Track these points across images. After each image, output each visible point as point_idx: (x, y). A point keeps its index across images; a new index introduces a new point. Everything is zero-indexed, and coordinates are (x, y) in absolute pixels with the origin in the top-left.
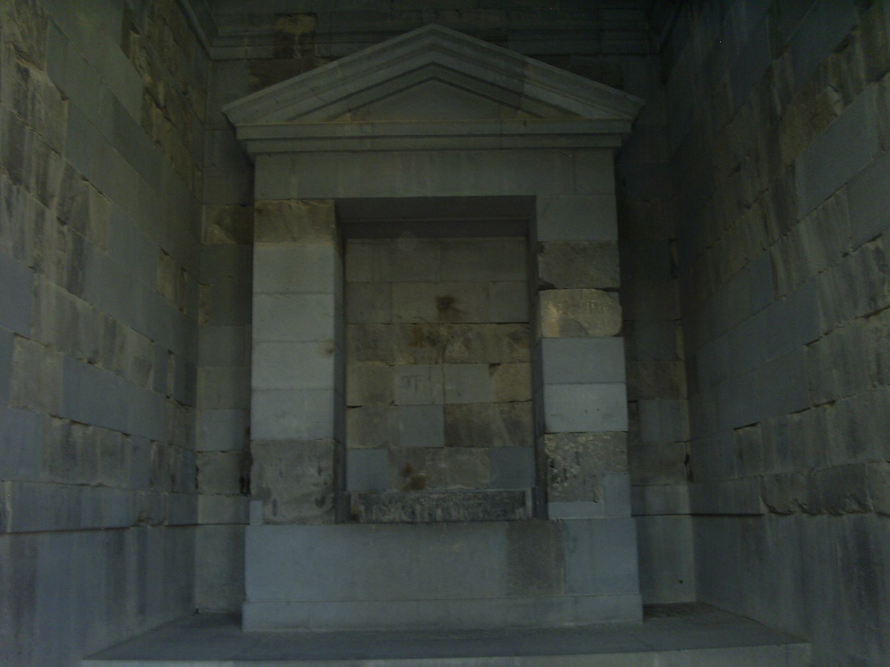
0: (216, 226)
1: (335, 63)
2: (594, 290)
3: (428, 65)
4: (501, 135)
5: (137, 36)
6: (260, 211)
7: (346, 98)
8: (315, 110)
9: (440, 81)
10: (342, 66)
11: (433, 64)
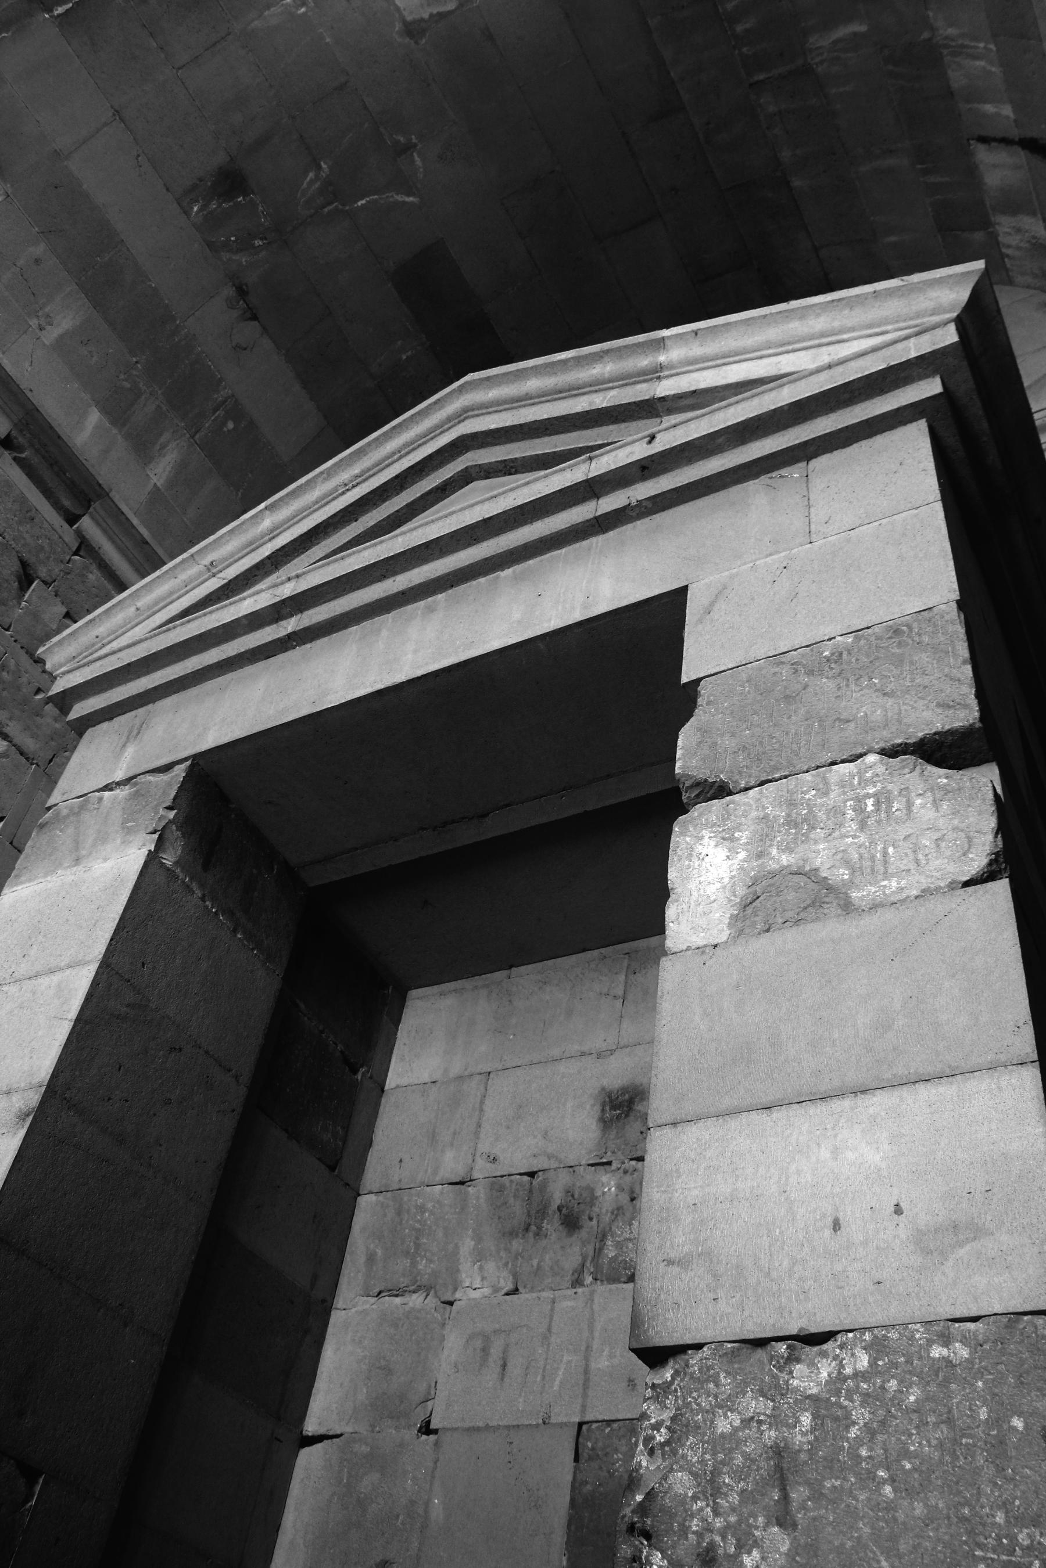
1: (263, 506)
2: (871, 758)
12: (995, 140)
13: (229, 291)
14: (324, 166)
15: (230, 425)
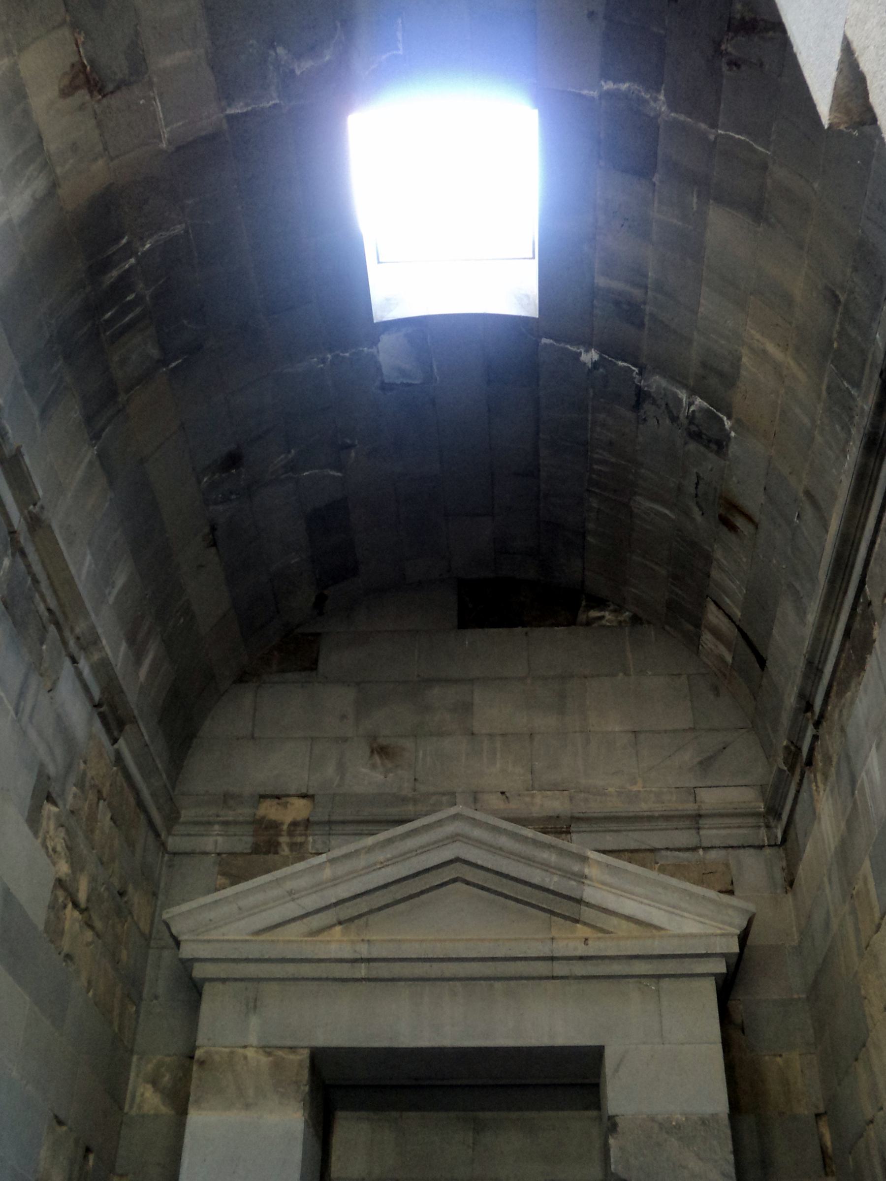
0: (149, 1086)
1: (323, 858)
3: (451, 862)
4: (552, 959)
5: (54, 809)
6: (202, 1063)
7: (336, 904)
8: (294, 920)
9: (468, 883)
10: (332, 861)
11: (457, 860)
12: (723, 611)
13: (207, 530)
14: (293, 451)
15: (182, 620)
